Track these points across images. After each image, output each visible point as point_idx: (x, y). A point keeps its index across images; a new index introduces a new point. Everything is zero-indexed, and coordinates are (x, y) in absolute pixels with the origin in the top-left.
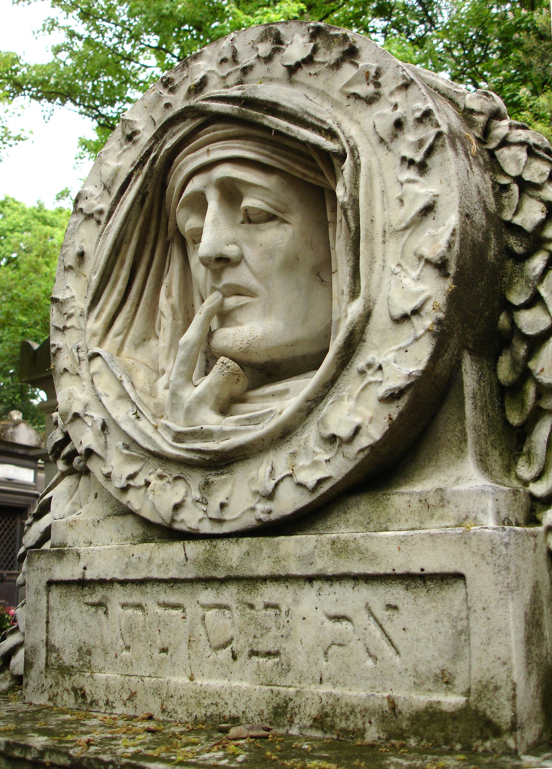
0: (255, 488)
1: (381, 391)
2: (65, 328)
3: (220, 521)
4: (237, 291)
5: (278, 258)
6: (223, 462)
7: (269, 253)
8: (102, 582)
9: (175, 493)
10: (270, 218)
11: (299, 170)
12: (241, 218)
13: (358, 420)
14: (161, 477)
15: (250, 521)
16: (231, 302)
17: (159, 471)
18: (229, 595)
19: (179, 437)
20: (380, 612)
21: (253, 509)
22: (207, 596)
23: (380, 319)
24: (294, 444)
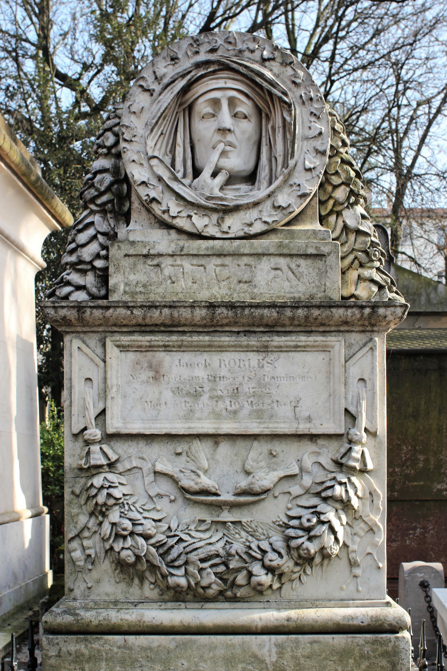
0: (244, 222)
1: (299, 193)
2: (131, 141)
3: (227, 233)
4: (230, 144)
5: (247, 135)
6: (228, 210)
7: (244, 132)
8: (160, 255)
9: (206, 220)
10: (246, 117)
11: (260, 103)
12: (233, 114)
13: (290, 202)
14: (196, 214)
15: (241, 234)
16: (228, 148)
17: (195, 211)
18: (228, 261)
19: (209, 198)
20: (293, 266)
21: (243, 230)
22: (219, 261)
23: (300, 167)
24: (260, 208)
